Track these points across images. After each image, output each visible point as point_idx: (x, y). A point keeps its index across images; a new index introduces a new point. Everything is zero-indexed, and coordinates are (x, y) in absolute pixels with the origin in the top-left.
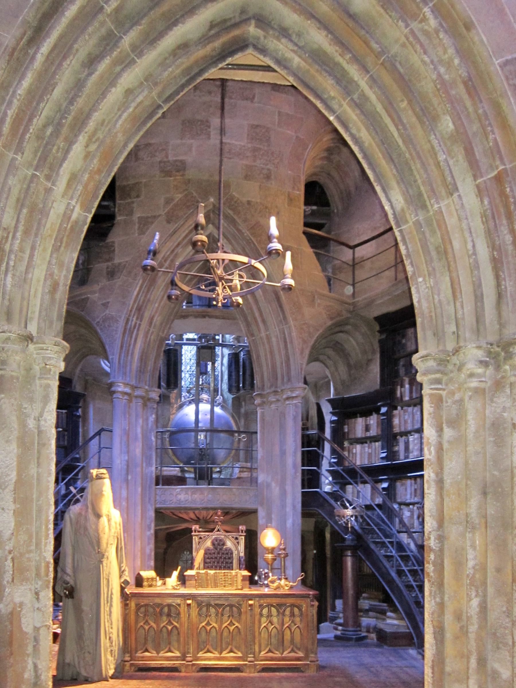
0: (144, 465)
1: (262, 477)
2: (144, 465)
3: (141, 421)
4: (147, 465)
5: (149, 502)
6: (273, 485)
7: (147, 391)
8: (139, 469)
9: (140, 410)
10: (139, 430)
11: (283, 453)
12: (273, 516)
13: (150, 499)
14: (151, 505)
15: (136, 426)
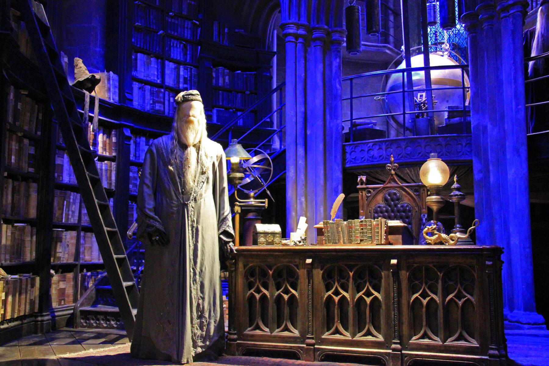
0: (328, 117)
1: (473, 120)
2: (328, 117)
3: (320, 66)
4: (331, 118)
5: (335, 161)
6: (489, 127)
7: (329, 34)
8: (320, 123)
9: (319, 54)
10: (319, 77)
11: (500, 84)
12: (491, 168)
13: (336, 157)
14: (338, 164)
15: (315, 72)
